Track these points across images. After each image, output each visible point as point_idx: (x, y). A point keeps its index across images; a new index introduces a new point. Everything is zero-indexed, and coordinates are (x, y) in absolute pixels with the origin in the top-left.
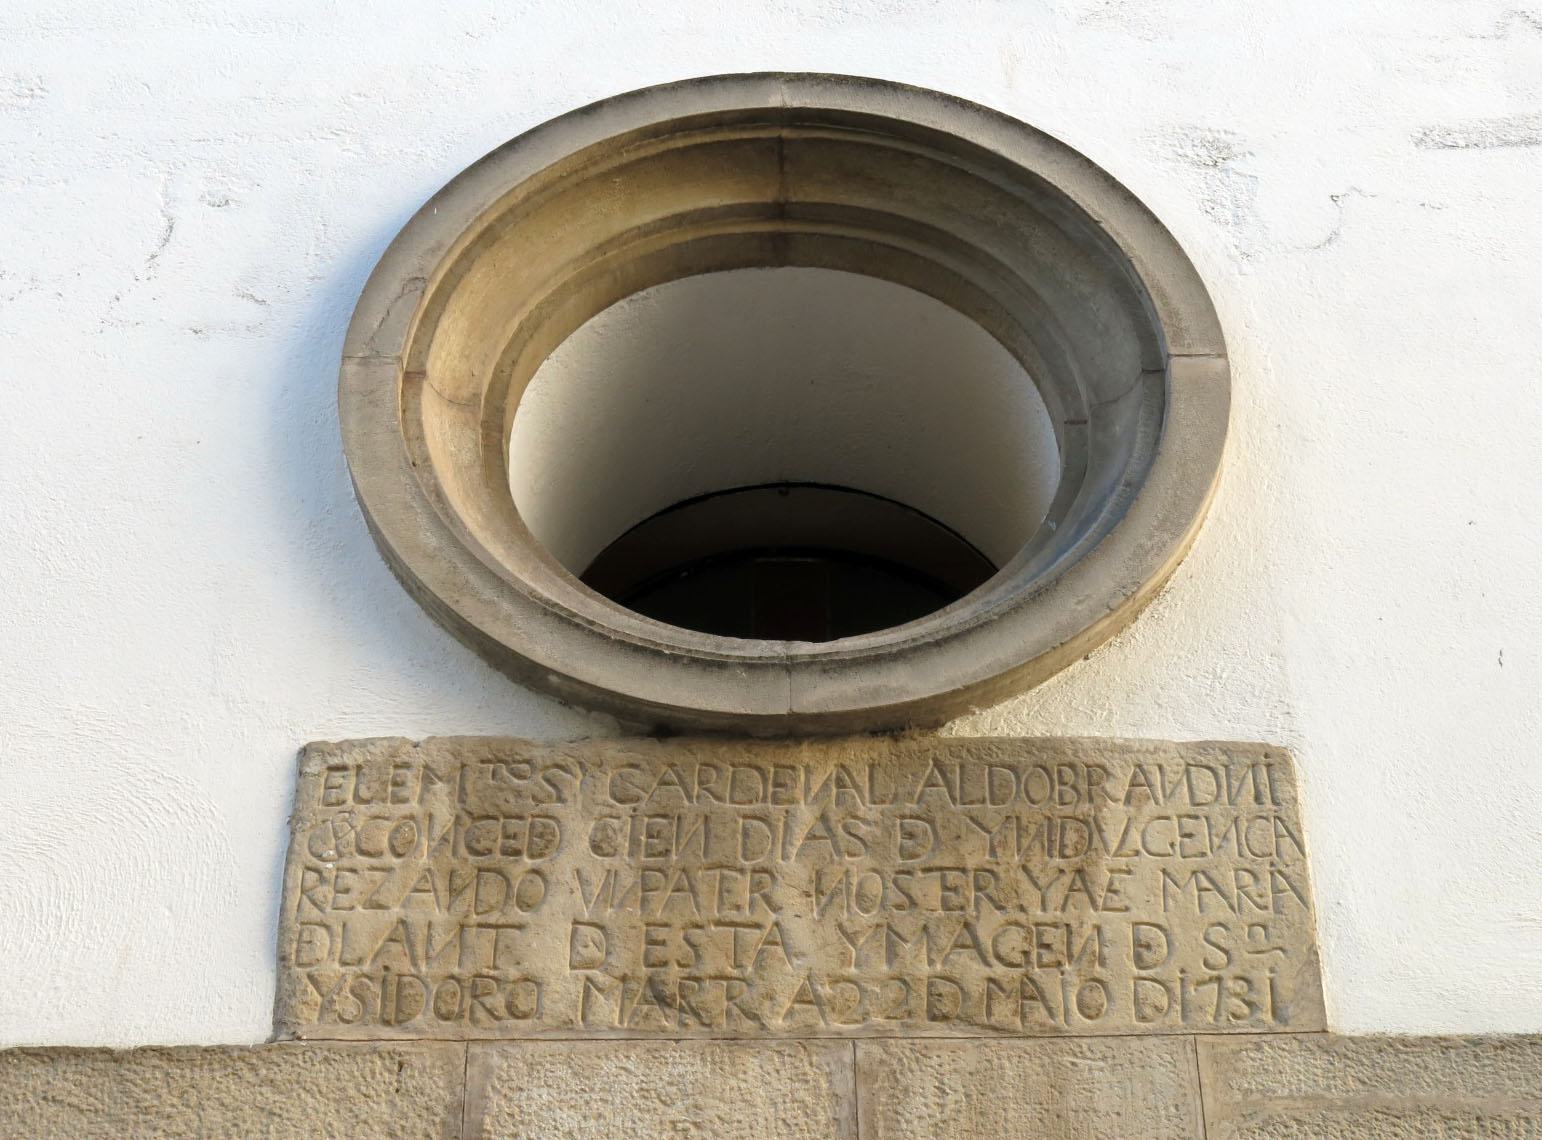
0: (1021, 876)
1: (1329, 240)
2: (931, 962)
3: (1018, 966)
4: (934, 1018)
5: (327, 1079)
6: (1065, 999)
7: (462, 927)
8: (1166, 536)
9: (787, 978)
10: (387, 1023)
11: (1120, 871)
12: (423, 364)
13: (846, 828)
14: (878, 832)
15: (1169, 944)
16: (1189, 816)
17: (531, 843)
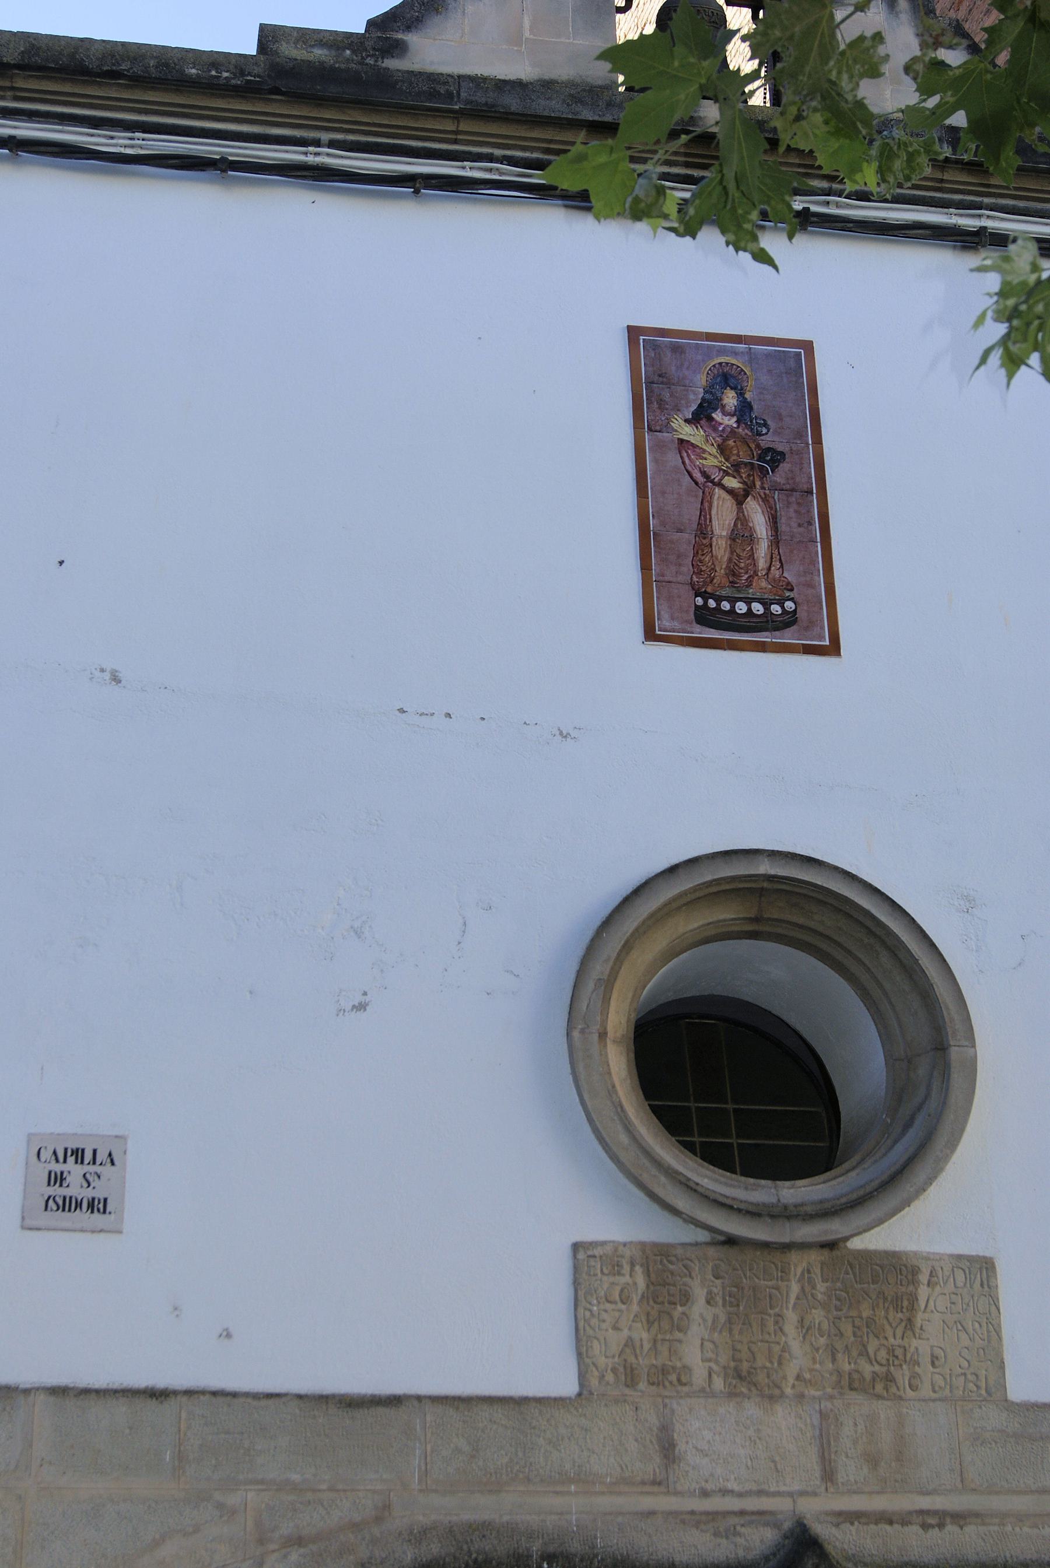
0: (885, 1322)
1: (1020, 964)
2: (850, 1363)
3: (885, 1365)
4: (851, 1389)
5: (607, 1413)
6: (904, 1382)
7: (655, 1341)
8: (948, 1151)
9: (792, 1369)
10: (627, 1386)
11: (926, 1320)
12: (605, 1029)
13: (812, 1295)
14: (826, 1298)
15: (945, 1357)
16: (954, 1293)
17: (680, 1299)
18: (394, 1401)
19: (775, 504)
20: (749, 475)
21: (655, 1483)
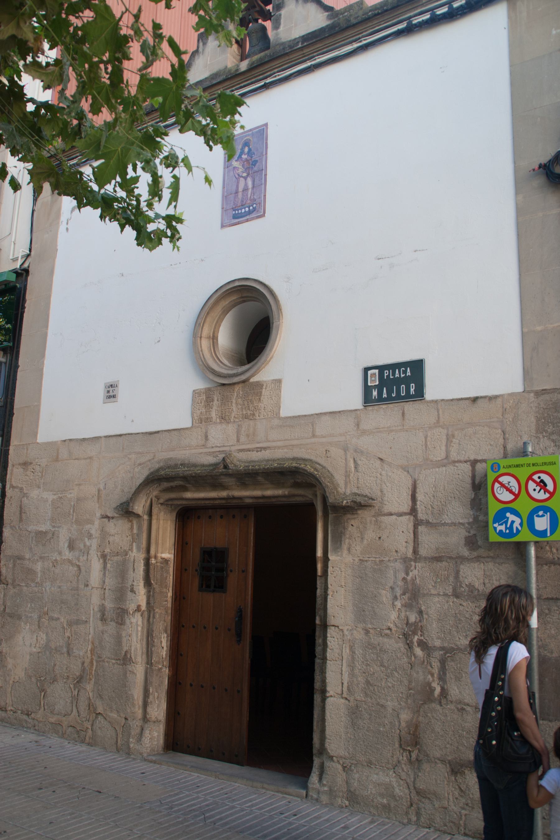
9: (233, 415)
18: (158, 432)
21: (203, 446)
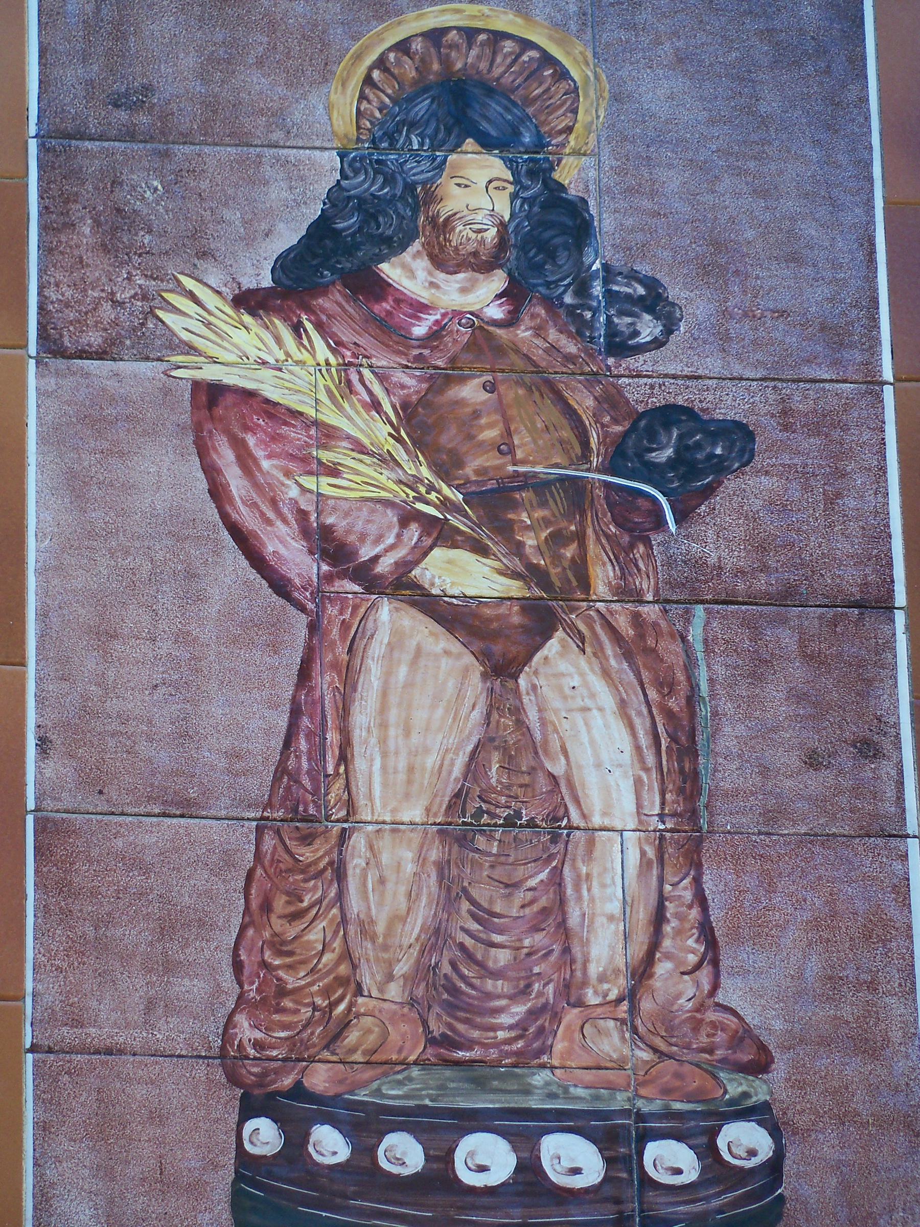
19: (690, 665)
20: (557, 539)
